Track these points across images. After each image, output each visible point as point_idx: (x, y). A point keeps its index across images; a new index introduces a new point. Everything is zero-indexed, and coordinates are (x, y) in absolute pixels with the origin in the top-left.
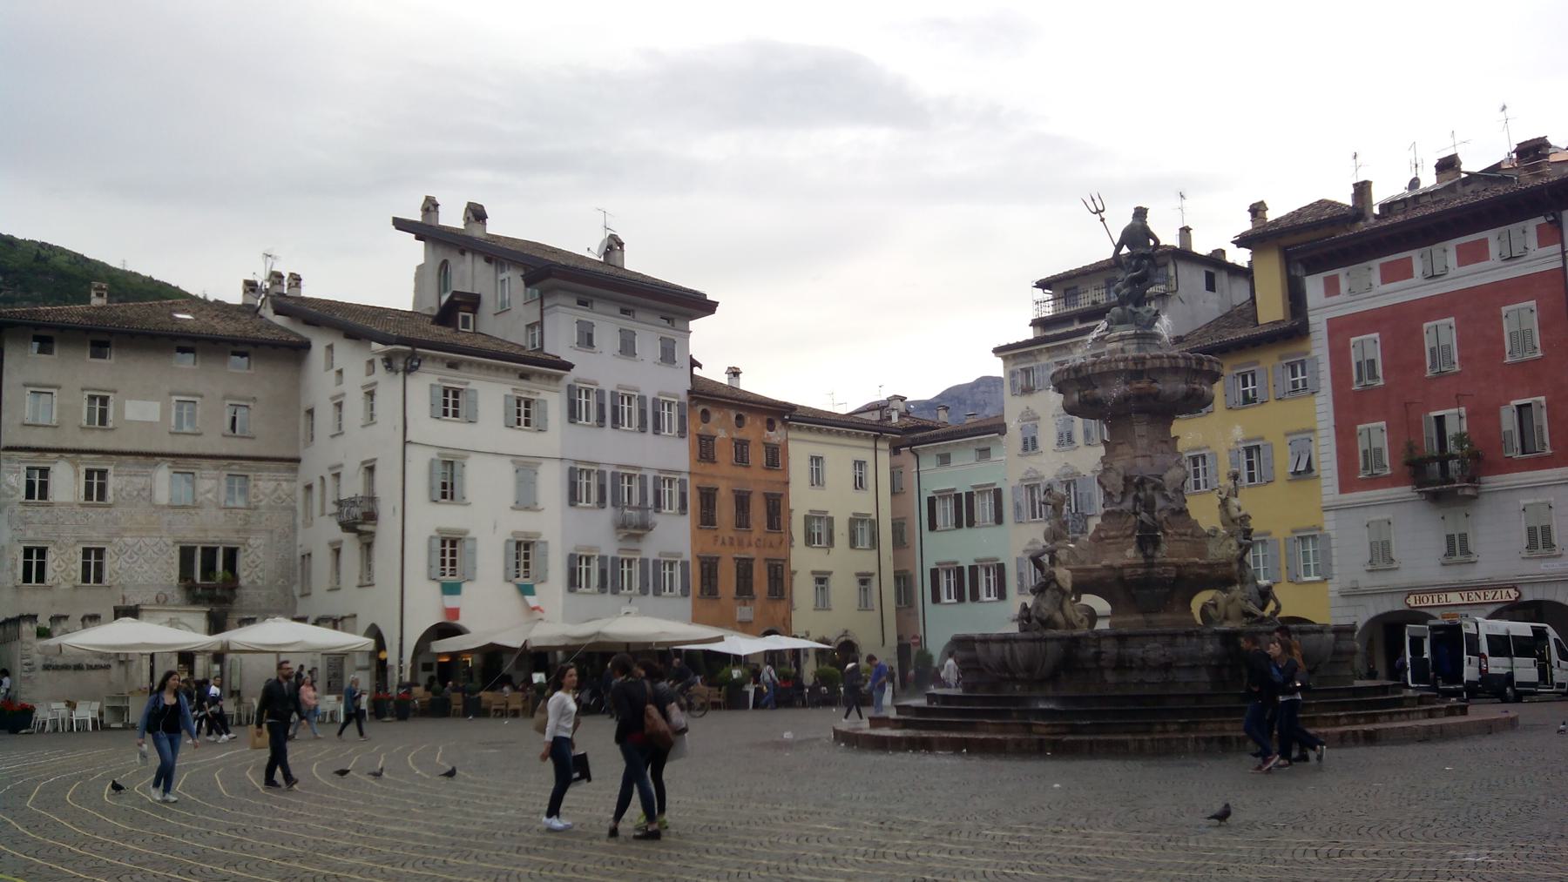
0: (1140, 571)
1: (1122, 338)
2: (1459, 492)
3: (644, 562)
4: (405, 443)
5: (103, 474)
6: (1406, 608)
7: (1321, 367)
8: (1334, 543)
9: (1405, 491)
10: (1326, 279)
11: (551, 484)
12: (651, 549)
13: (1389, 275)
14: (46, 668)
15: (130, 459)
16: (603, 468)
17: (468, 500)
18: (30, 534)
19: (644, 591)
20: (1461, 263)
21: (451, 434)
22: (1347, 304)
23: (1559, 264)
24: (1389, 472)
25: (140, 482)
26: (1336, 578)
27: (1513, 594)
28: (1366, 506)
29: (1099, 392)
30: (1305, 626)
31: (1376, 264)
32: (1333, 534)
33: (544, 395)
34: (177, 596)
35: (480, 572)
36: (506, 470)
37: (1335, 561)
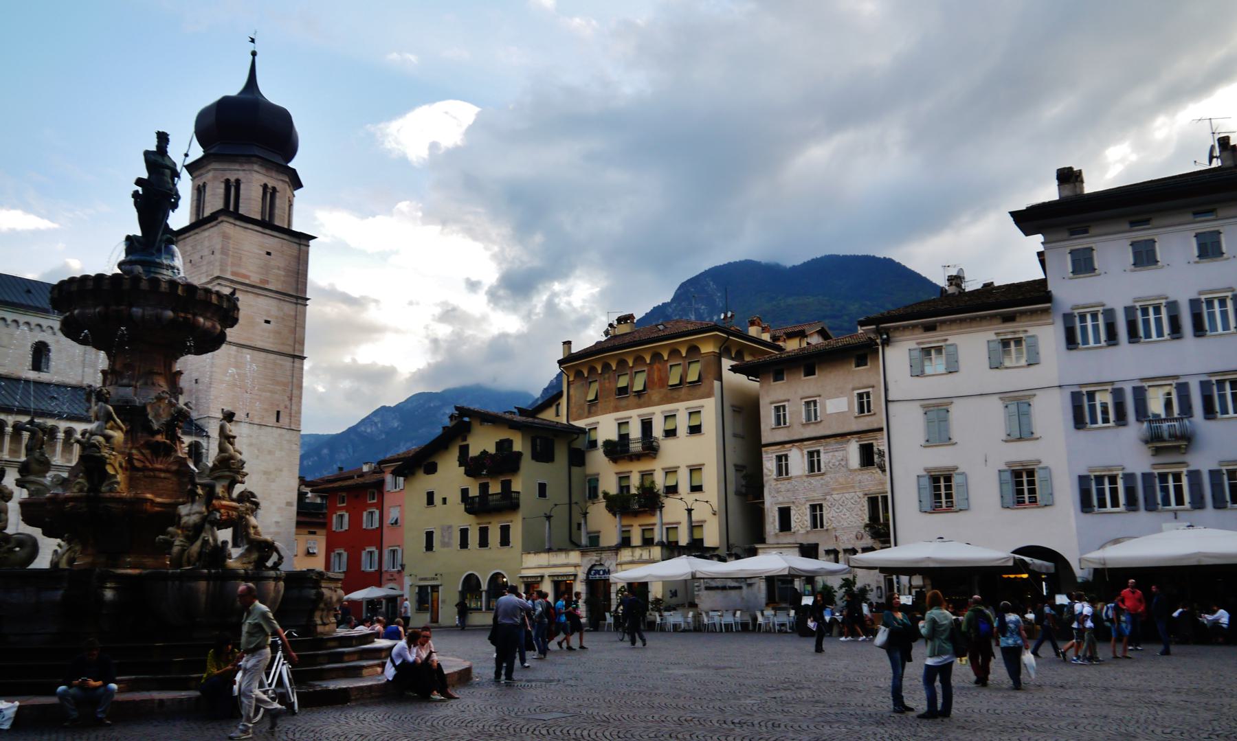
3: (1195, 476)
4: (887, 401)
5: (818, 452)
11: (1051, 413)
12: (1203, 461)
14: (708, 588)
15: (832, 440)
16: (1117, 386)
17: (954, 440)
18: (781, 499)
19: (1198, 503)
21: (936, 385)
25: (839, 455)
33: (1033, 331)
34: (567, 544)
35: (973, 501)
36: (996, 405)
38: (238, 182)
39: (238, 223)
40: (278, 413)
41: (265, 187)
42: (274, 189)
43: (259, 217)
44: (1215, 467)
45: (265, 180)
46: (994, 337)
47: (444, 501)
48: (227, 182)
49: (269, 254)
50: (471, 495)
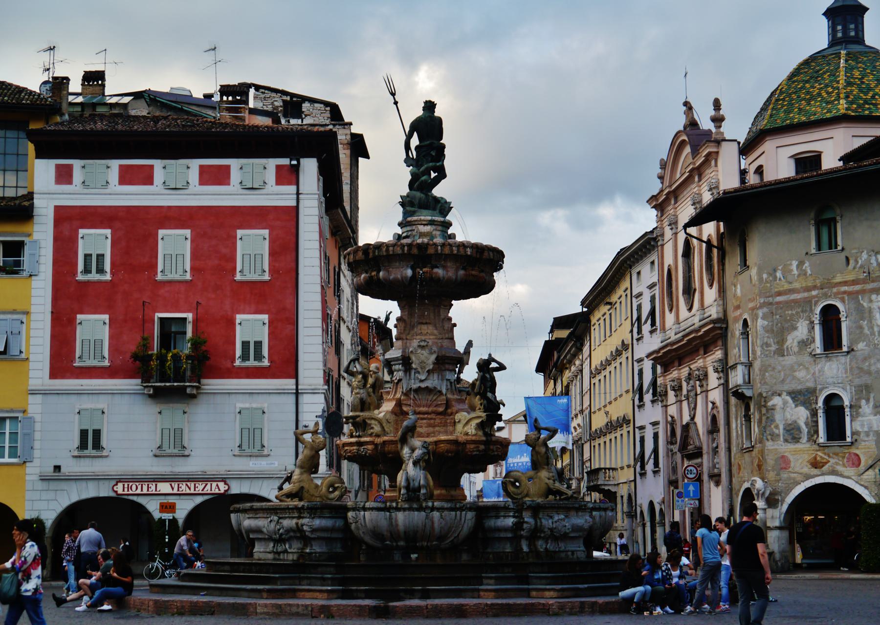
0: (482, 447)
1: (431, 223)
2: (188, 391)
6: (113, 494)
7: (43, 252)
8: (38, 426)
9: (133, 384)
10: (58, 167)
13: (127, 177)
20: (202, 182)
22: (76, 196)
23: (294, 203)
24: (106, 363)
26: (37, 462)
27: (223, 487)
28: (79, 393)
29: (440, 272)
30: (264, 504)
31: (115, 164)
32: (38, 418)
37: (37, 445)
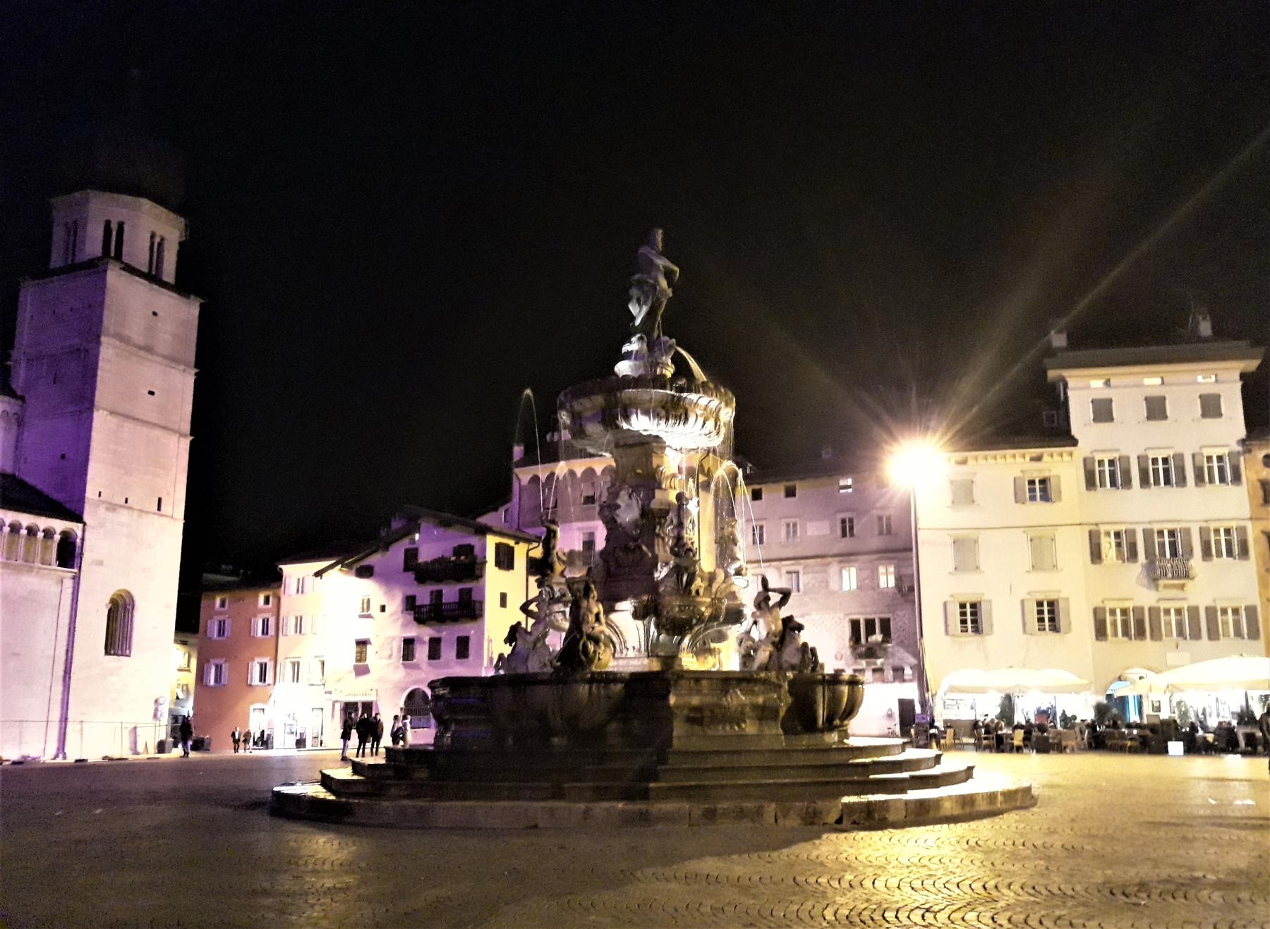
11: (1073, 547)
17: (982, 568)
19: (1196, 635)
38: (121, 226)
39: (123, 272)
40: (160, 500)
41: (153, 236)
42: (162, 239)
43: (145, 270)
44: (1211, 603)
45: (154, 228)
46: (1019, 474)
47: (383, 609)
48: (108, 223)
49: (155, 314)
50: (418, 603)
